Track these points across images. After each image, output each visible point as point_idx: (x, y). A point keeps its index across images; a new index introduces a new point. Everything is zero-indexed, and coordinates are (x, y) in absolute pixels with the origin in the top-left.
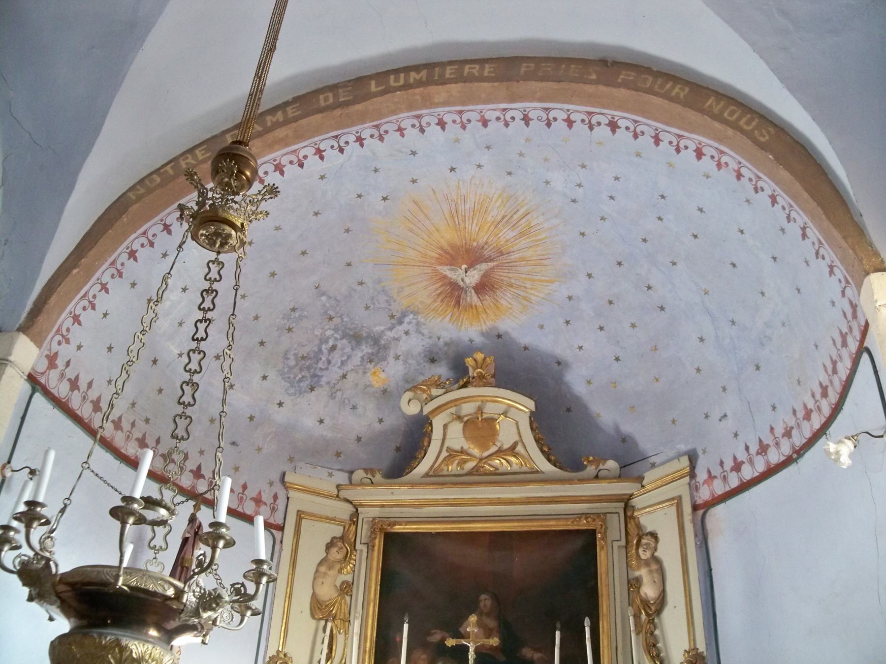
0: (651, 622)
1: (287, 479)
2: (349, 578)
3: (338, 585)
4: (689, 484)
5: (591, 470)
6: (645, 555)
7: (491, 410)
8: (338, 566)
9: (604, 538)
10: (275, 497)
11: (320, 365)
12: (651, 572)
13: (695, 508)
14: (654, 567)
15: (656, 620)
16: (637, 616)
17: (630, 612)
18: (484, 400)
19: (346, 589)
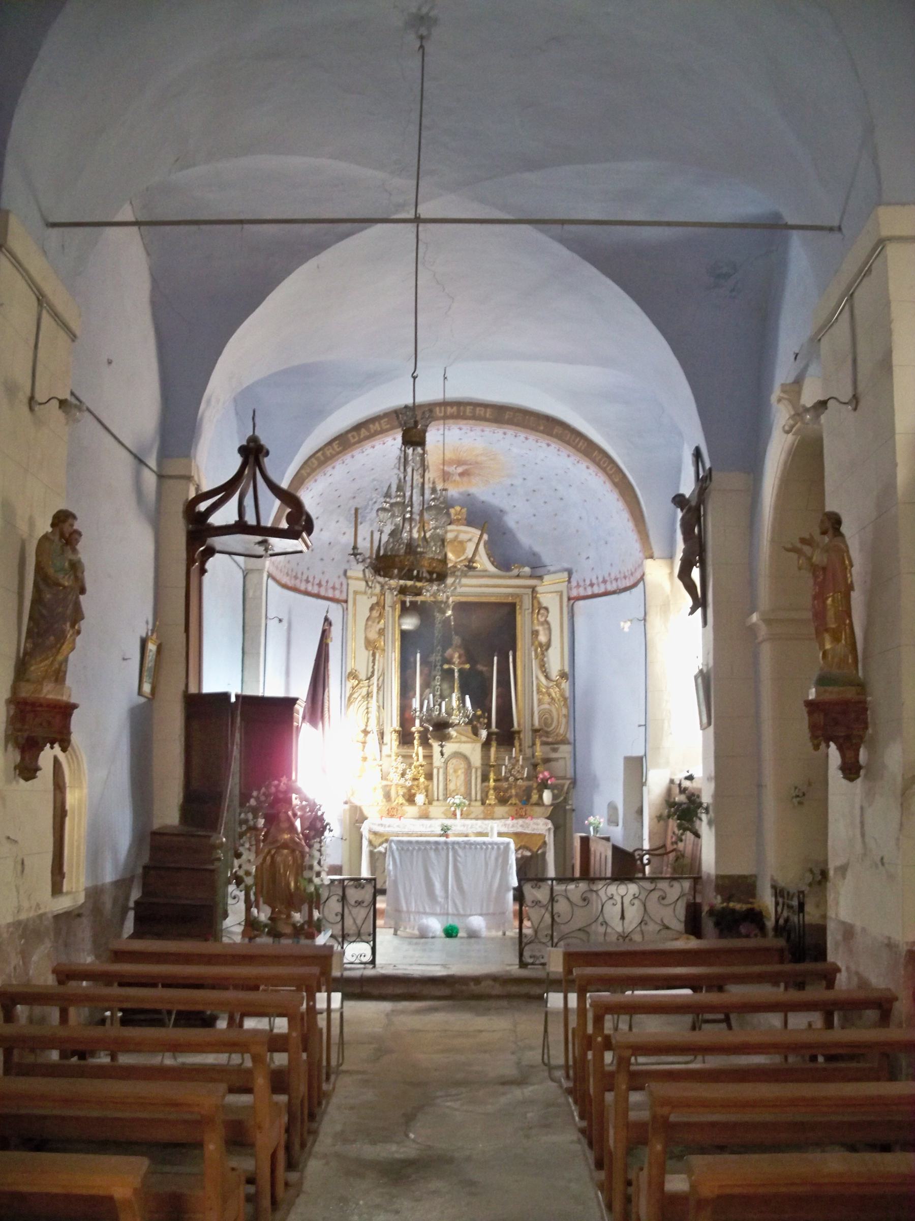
0: (543, 654)
1: (349, 573)
2: (383, 627)
3: (377, 629)
4: (567, 586)
5: (515, 572)
6: (542, 619)
7: (462, 537)
8: (377, 621)
9: (521, 608)
10: (341, 584)
11: (367, 511)
12: (544, 629)
13: (569, 599)
14: (546, 626)
15: (545, 653)
16: (536, 651)
17: (533, 649)
18: (459, 532)
19: (381, 632)
